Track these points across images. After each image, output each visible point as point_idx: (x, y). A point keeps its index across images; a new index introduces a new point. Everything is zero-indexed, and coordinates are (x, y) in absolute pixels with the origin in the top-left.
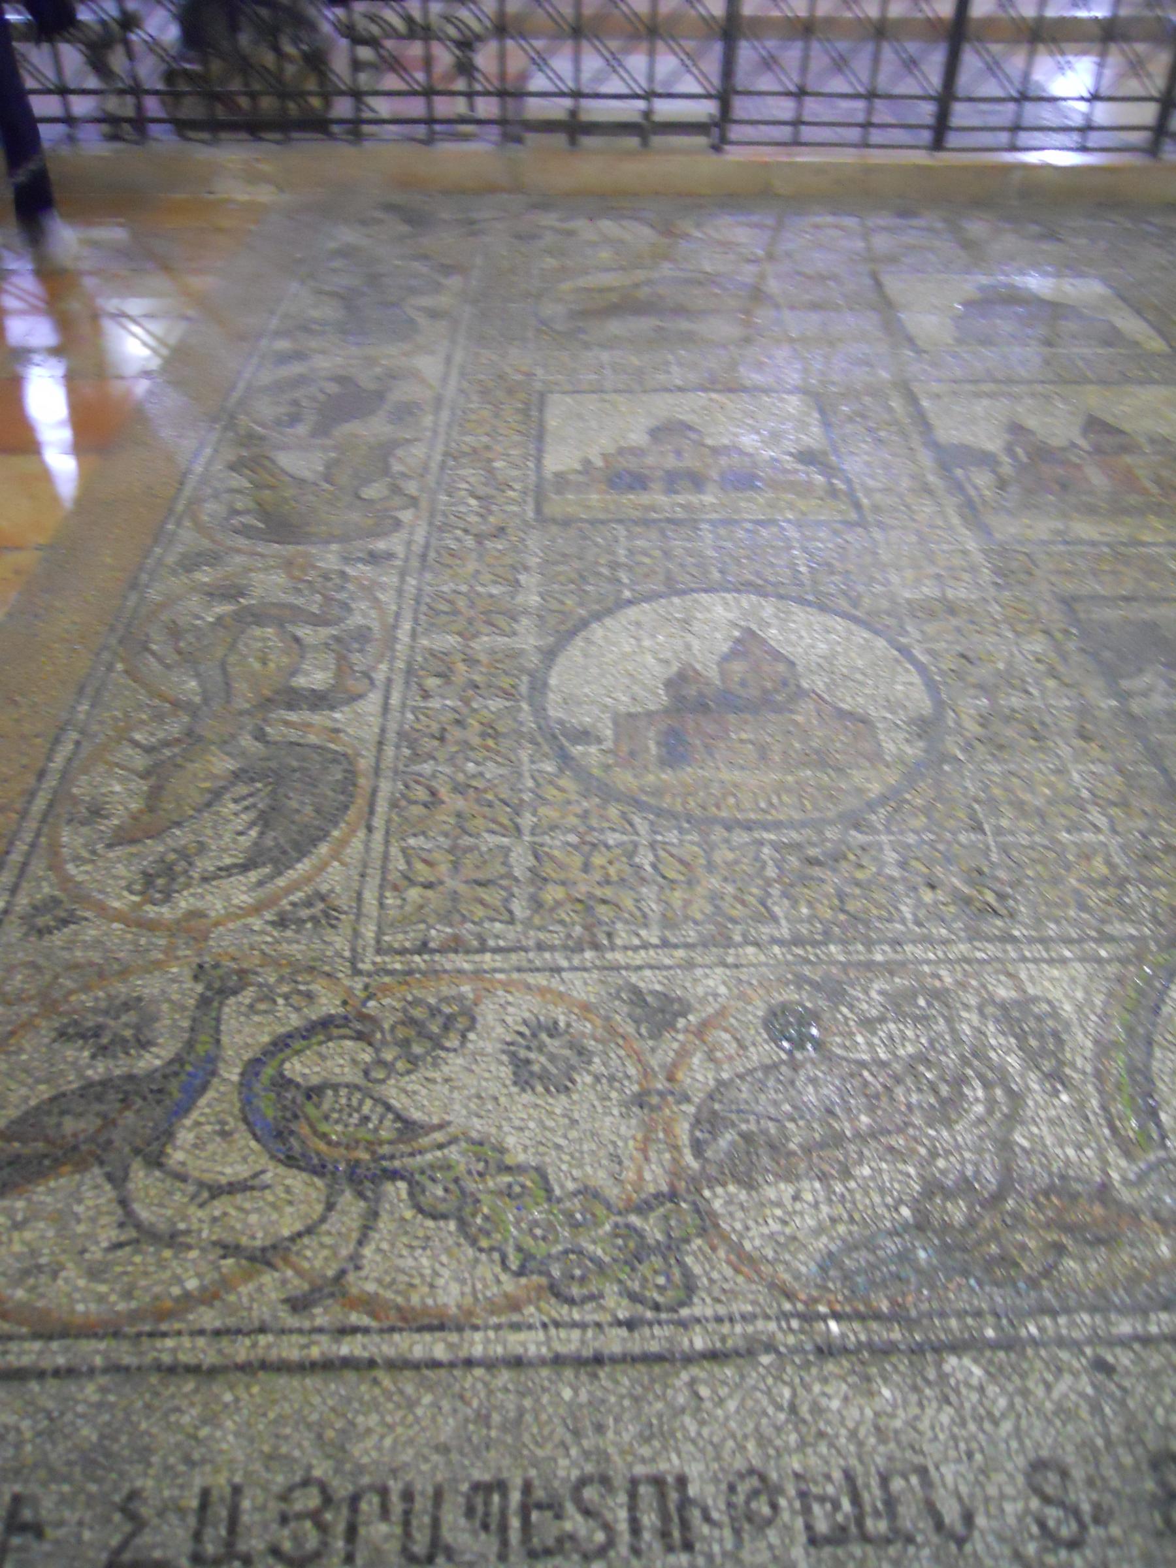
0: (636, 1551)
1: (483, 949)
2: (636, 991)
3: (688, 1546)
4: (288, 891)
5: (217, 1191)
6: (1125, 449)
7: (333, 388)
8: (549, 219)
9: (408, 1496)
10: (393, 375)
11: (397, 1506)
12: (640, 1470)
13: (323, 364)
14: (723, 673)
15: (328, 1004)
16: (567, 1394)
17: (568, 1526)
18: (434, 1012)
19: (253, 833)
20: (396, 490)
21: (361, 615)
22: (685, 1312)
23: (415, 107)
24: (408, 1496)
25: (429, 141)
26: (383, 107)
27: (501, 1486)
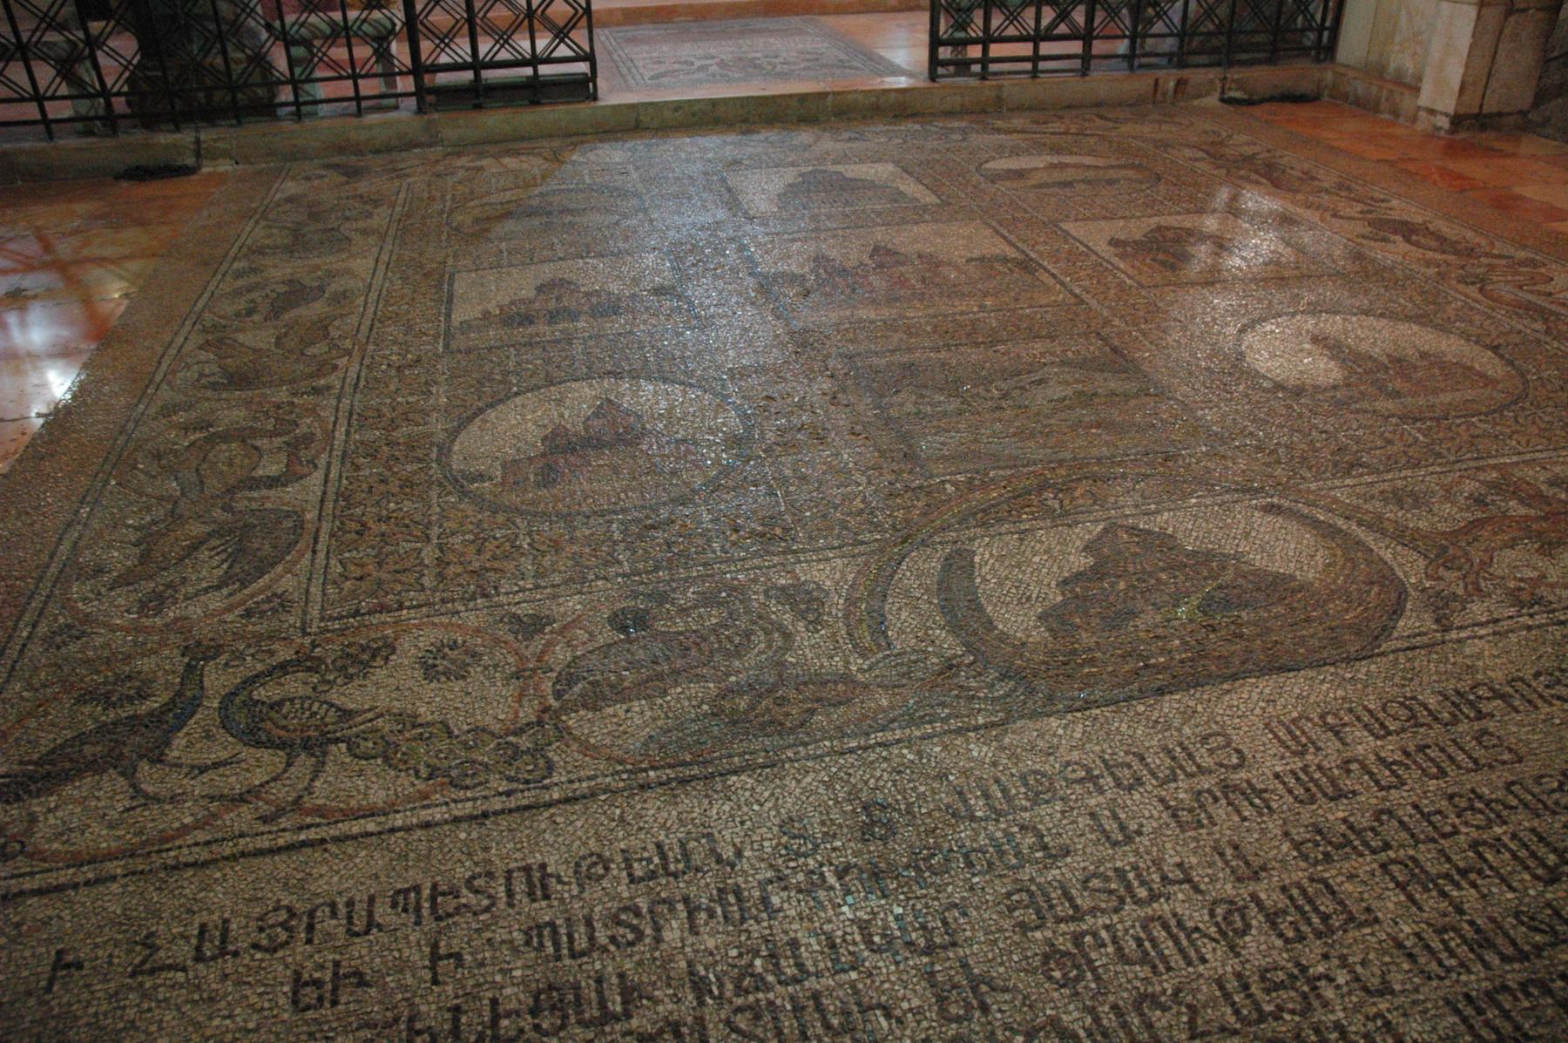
0: (511, 905)
1: (401, 607)
2: (514, 615)
3: (547, 897)
4: (252, 596)
5: (203, 770)
6: (898, 263)
7: (282, 289)
8: (463, 161)
9: (350, 903)
10: (332, 275)
11: (342, 910)
12: (513, 865)
13: (277, 274)
14: (586, 430)
15: (284, 654)
16: (463, 836)
17: (463, 901)
18: (363, 649)
19: (225, 566)
20: (333, 346)
21: (306, 425)
22: (546, 781)
23: (346, 88)
24: (350, 903)
25: (360, 112)
26: (321, 91)
27: (417, 889)
